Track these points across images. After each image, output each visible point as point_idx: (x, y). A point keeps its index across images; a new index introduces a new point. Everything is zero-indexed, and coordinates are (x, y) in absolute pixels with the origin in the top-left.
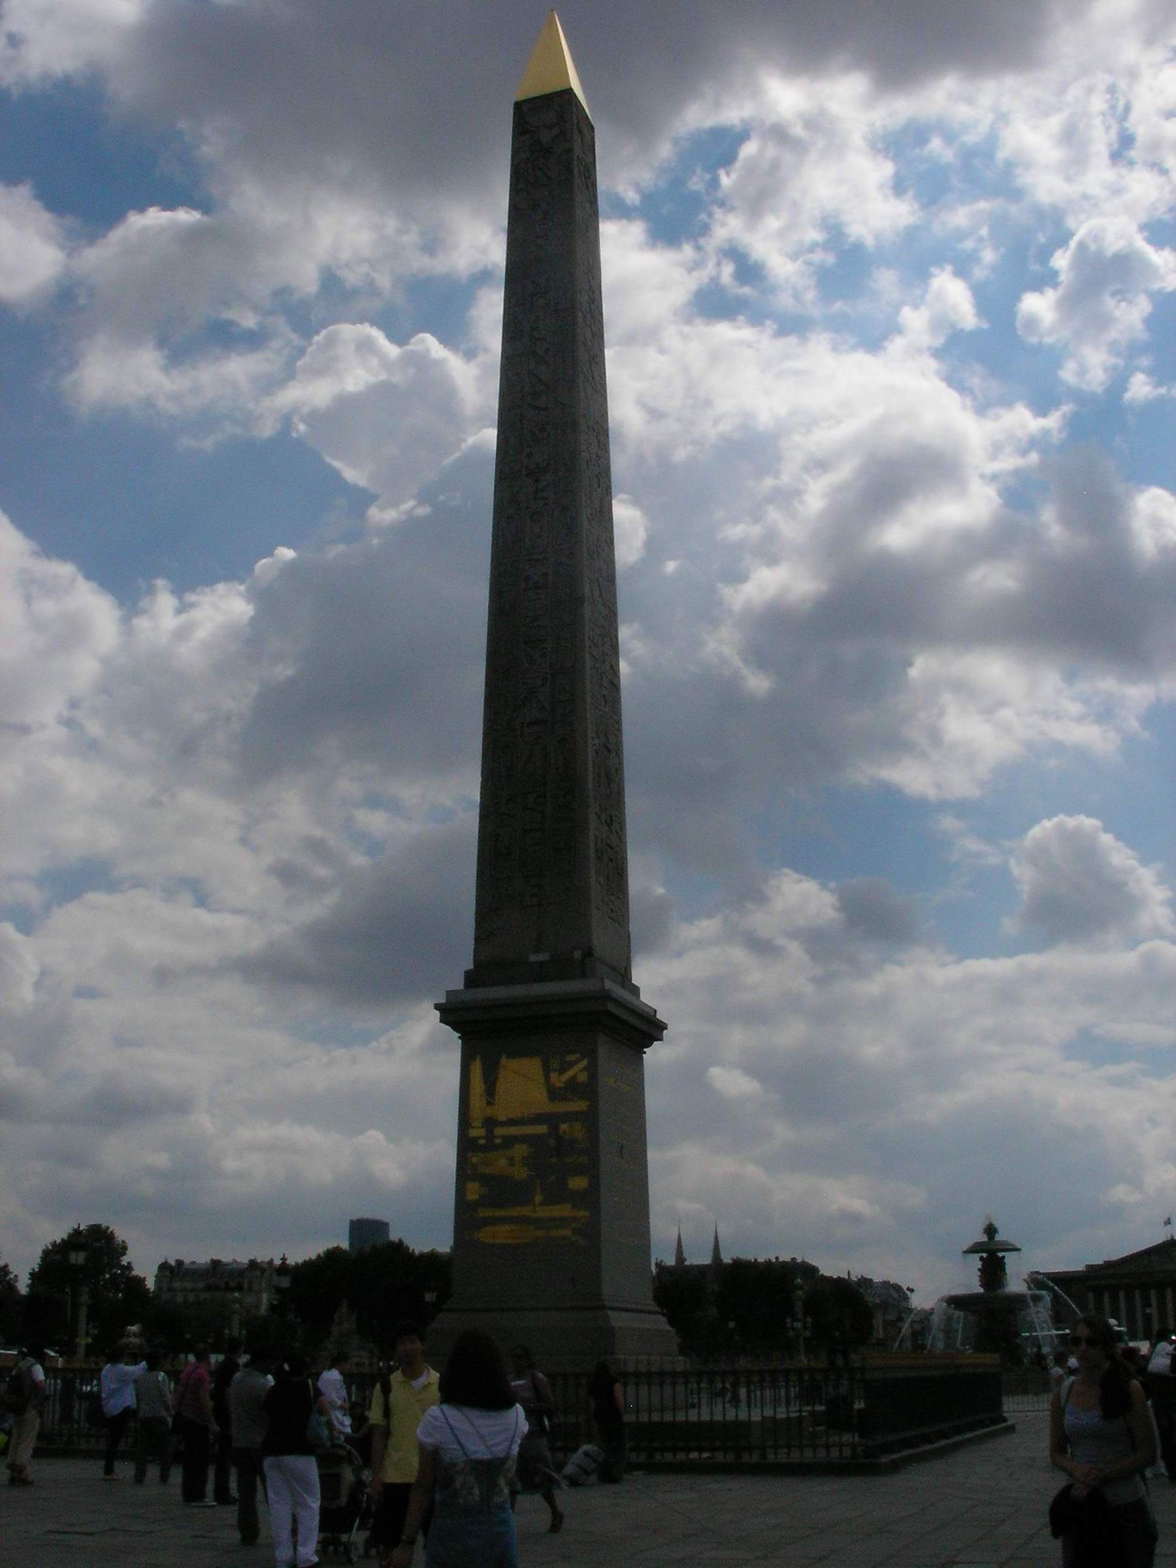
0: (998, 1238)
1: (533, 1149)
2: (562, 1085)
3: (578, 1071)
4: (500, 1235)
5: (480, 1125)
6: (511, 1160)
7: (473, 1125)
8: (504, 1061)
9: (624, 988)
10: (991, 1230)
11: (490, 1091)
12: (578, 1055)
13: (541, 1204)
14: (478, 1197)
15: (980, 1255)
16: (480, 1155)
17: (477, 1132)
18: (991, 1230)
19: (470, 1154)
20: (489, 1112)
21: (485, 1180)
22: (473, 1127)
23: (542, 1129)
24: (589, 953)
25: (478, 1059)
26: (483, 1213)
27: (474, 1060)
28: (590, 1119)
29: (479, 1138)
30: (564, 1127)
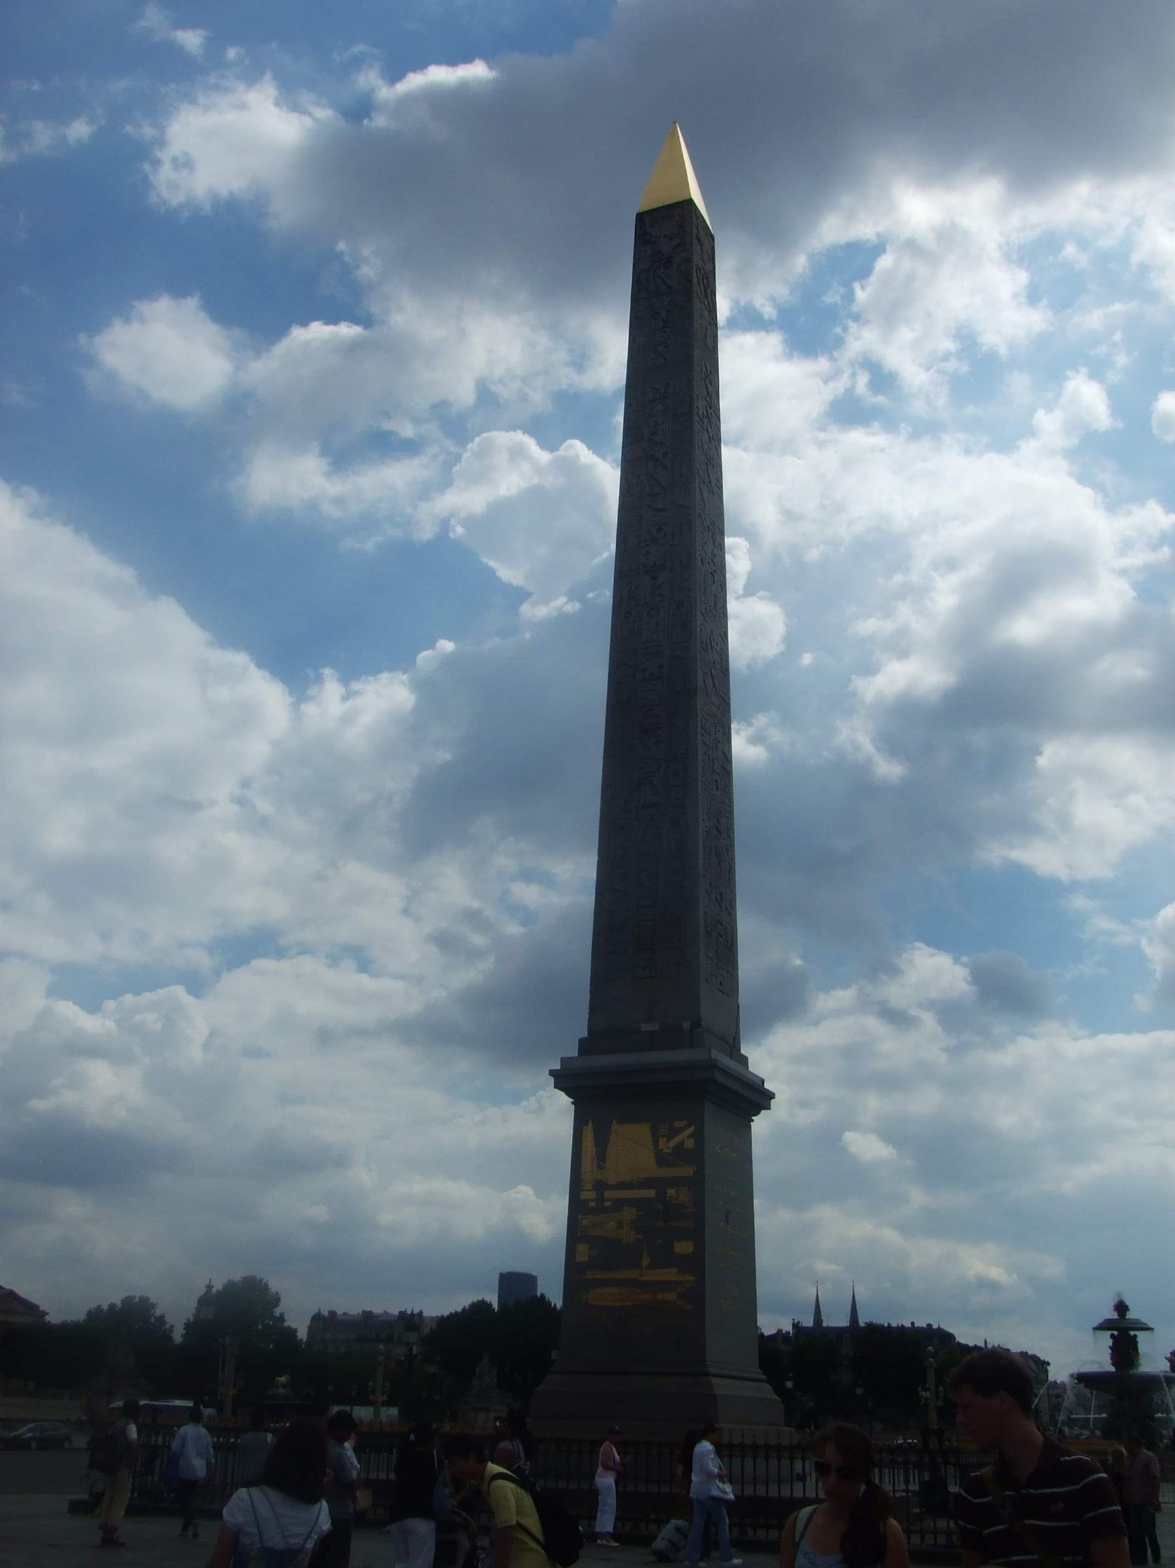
0: (1131, 1315)
2: (670, 1151)
3: (685, 1137)
6: (620, 1225)
7: (584, 1188)
8: (615, 1126)
9: (731, 1057)
10: (1121, 1308)
11: (601, 1156)
12: (686, 1122)
13: (646, 1269)
15: (1110, 1332)
18: (1121, 1308)
22: (583, 1190)
23: (650, 1193)
24: (697, 1023)
25: (590, 1122)
27: (587, 1124)
28: (697, 1185)
29: (592, 1200)
30: (671, 1192)
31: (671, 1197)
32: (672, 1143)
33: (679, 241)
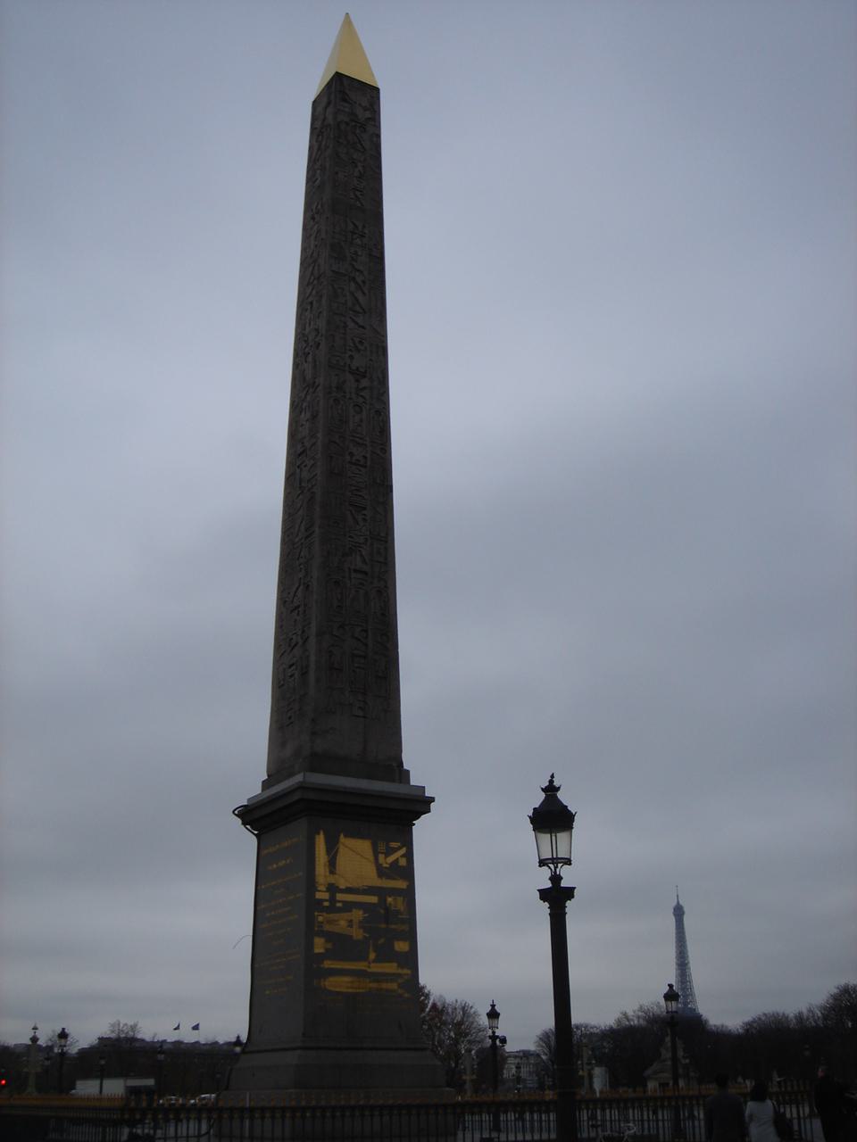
1: (366, 915)
2: (388, 866)
4: (339, 984)
5: (325, 889)
7: (319, 889)
8: (342, 838)
11: (332, 864)
12: (399, 844)
13: (374, 961)
14: (322, 951)
16: (324, 914)
17: (322, 895)
19: (316, 914)
20: (331, 879)
21: (329, 936)
22: (319, 891)
23: (374, 899)
24: (401, 764)
25: (322, 833)
26: (327, 964)
27: (319, 834)
28: (409, 895)
29: (326, 900)
30: (390, 900)
31: (390, 904)
32: (391, 859)
33: (370, 116)
